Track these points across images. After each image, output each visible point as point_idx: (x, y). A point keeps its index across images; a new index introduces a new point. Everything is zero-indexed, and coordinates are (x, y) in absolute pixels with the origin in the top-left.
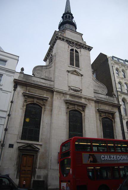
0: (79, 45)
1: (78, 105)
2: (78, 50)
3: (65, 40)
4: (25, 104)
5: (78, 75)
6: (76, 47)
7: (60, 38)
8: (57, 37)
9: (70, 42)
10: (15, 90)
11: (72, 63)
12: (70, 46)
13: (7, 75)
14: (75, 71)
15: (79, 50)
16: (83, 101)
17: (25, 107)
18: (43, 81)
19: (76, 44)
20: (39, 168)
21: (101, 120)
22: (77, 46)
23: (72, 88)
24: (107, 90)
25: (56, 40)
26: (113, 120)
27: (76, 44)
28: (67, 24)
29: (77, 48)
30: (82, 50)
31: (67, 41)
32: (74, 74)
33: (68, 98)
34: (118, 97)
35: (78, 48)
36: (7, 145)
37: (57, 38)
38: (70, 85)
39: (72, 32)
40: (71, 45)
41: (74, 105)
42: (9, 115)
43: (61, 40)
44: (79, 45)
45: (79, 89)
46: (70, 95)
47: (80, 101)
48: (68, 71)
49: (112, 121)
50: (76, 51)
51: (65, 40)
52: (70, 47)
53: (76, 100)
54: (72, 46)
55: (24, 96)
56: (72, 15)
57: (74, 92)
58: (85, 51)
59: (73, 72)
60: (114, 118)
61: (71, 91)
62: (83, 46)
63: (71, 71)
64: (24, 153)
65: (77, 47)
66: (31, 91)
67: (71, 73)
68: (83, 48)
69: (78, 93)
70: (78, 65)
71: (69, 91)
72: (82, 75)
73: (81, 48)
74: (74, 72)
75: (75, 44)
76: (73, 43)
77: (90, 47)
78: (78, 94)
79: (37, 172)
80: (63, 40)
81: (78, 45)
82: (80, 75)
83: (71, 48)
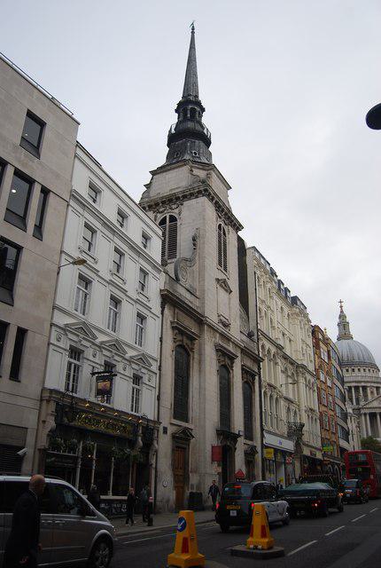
5: (226, 291)
8: (206, 190)
9: (220, 206)
10: (162, 313)
11: (220, 264)
13: (156, 278)
18: (188, 295)
20: (191, 472)
25: (200, 192)
28: (202, 144)
36: (161, 430)
46: (220, 334)
47: (226, 347)
48: (218, 280)
55: (173, 328)
60: (253, 383)
64: (180, 445)
66: (180, 318)
70: (225, 269)
76: (223, 211)
77: (240, 225)
79: (191, 479)
80: (212, 199)
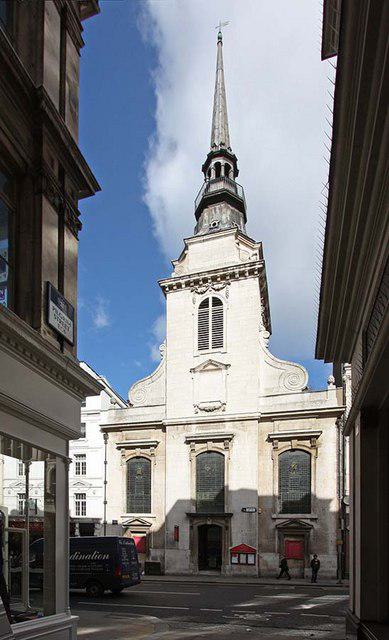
0: (223, 277)
1: (214, 441)
2: (220, 295)
3: (183, 286)
4: (125, 460)
8: (164, 288)
9: (196, 282)
14: (211, 362)
16: (228, 428)
17: (125, 466)
19: (214, 279)
21: (277, 458)
24: (307, 376)
26: (313, 452)
27: (214, 279)
30: (235, 287)
31: (188, 284)
32: (208, 371)
33: (194, 431)
35: (218, 290)
41: (205, 441)
42: (106, 483)
44: (223, 277)
45: (218, 405)
48: (193, 370)
49: (310, 454)
51: (183, 286)
53: (211, 431)
56: (233, 159)
62: (233, 276)
65: (216, 287)
66: (129, 436)
67: (201, 371)
68: (237, 280)
69: (218, 413)
76: (205, 280)
78: (217, 416)
80: (179, 286)
82: (222, 367)
83: (200, 299)
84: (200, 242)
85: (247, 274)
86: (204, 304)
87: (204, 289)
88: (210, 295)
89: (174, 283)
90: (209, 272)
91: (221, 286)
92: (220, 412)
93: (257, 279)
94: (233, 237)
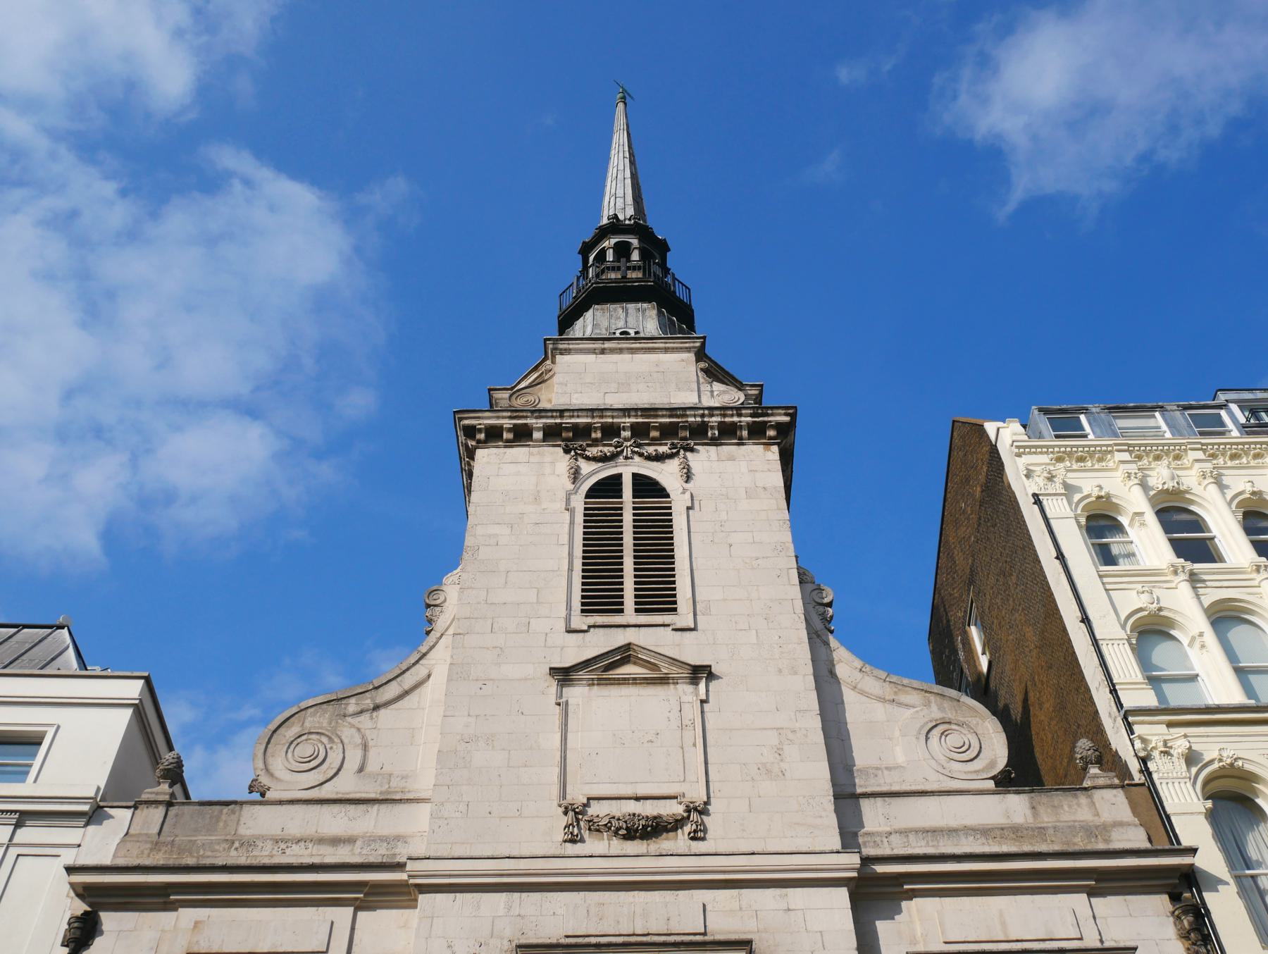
0: (668, 432)
2: (667, 474)
3: (538, 435)
5: (664, 680)
6: (641, 455)
7: (494, 435)
8: (470, 432)
9: (582, 432)
12: (588, 458)
15: (673, 466)
22: (654, 442)
23: (595, 810)
27: (640, 432)
29: (649, 458)
30: (704, 459)
31: (551, 434)
32: (624, 681)
34: (1146, 771)
35: (659, 458)
37: (472, 437)
38: (577, 795)
39: (612, 351)
40: (593, 451)
43: (509, 444)
44: (668, 432)
48: (564, 675)
50: (647, 487)
51: (538, 435)
52: (586, 467)
54: (604, 459)
57: (617, 846)
58: (732, 458)
59: (608, 668)
61: (594, 844)
62: (699, 432)
63: (586, 664)
68: (715, 442)
71: (571, 849)
72: (700, 673)
73: (692, 450)
74: (625, 661)
75: (626, 434)
76: (611, 431)
80: (522, 435)
81: (654, 434)
83: (593, 473)
84: (593, 351)
85: (745, 433)
86: (610, 487)
87: (608, 450)
88: (627, 469)
89: (507, 423)
90: (626, 412)
91: (663, 449)
92: (681, 840)
93: (775, 449)
94: (691, 357)
